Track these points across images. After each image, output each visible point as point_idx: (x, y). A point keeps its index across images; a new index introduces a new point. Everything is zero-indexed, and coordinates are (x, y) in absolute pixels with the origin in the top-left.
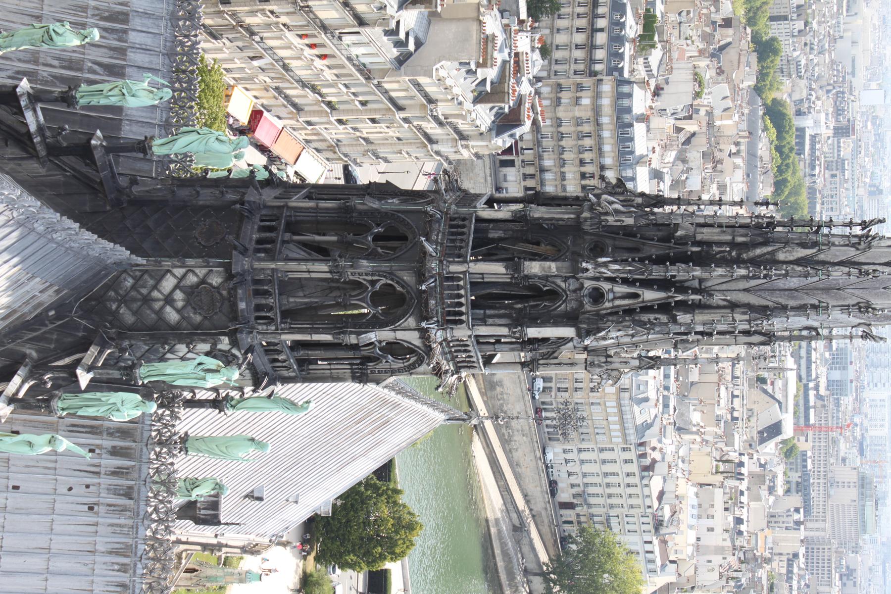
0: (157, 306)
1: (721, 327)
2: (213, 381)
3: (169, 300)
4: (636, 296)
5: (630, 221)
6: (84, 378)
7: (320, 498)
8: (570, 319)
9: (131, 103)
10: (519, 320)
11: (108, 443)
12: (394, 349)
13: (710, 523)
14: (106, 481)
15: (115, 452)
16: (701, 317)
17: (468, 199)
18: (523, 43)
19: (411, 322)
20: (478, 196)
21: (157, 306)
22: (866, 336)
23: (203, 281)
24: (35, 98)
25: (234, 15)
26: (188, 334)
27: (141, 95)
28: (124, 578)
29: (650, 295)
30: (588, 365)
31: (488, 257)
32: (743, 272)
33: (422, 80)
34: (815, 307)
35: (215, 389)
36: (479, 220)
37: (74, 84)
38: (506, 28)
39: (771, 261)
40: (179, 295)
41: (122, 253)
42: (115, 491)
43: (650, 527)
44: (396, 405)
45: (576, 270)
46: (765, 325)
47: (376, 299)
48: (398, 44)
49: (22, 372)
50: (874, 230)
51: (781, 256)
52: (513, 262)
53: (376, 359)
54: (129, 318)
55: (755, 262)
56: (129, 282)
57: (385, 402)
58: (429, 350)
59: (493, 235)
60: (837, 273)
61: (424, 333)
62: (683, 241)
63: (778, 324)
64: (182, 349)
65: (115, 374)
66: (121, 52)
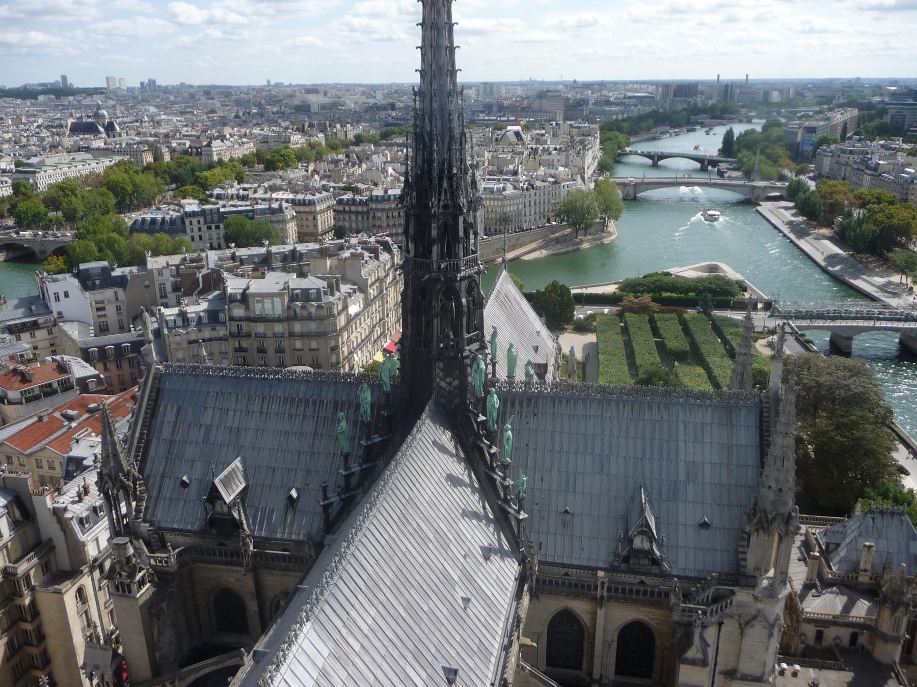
0: (452, 389)
1: (458, 154)
2: (483, 366)
3: (450, 384)
4: (446, 191)
5: (414, 194)
6: (482, 418)
7: (536, 323)
9: (369, 399)
11: (509, 408)
12: (469, 291)
13: (556, 161)
14: (524, 409)
15: (513, 406)
16: (454, 163)
18: (354, 241)
19: (457, 284)
20: (406, 257)
21: (452, 389)
23: (442, 370)
24: (368, 438)
25: (344, 360)
26: (463, 376)
27: (366, 396)
28: (564, 402)
29: (445, 185)
30: (475, 210)
31: (431, 253)
32: (435, 145)
33: (369, 282)
34: (450, 115)
35: (487, 365)
36: (415, 256)
37: (362, 422)
38: (348, 248)
39: (430, 134)
40: (448, 380)
41: (431, 403)
42: (529, 405)
43: (557, 186)
44: (499, 291)
46: (457, 136)
47: (449, 299)
48: (355, 292)
49: (479, 443)
51: (429, 129)
52: (432, 242)
53: (474, 298)
54: (458, 400)
55: (431, 140)
56: (443, 400)
57: (497, 296)
58: (470, 277)
59: (421, 250)
60: (435, 106)
61: (462, 279)
62: (423, 171)
63: (457, 131)
64: (470, 379)
65: (480, 406)
66: (350, 404)
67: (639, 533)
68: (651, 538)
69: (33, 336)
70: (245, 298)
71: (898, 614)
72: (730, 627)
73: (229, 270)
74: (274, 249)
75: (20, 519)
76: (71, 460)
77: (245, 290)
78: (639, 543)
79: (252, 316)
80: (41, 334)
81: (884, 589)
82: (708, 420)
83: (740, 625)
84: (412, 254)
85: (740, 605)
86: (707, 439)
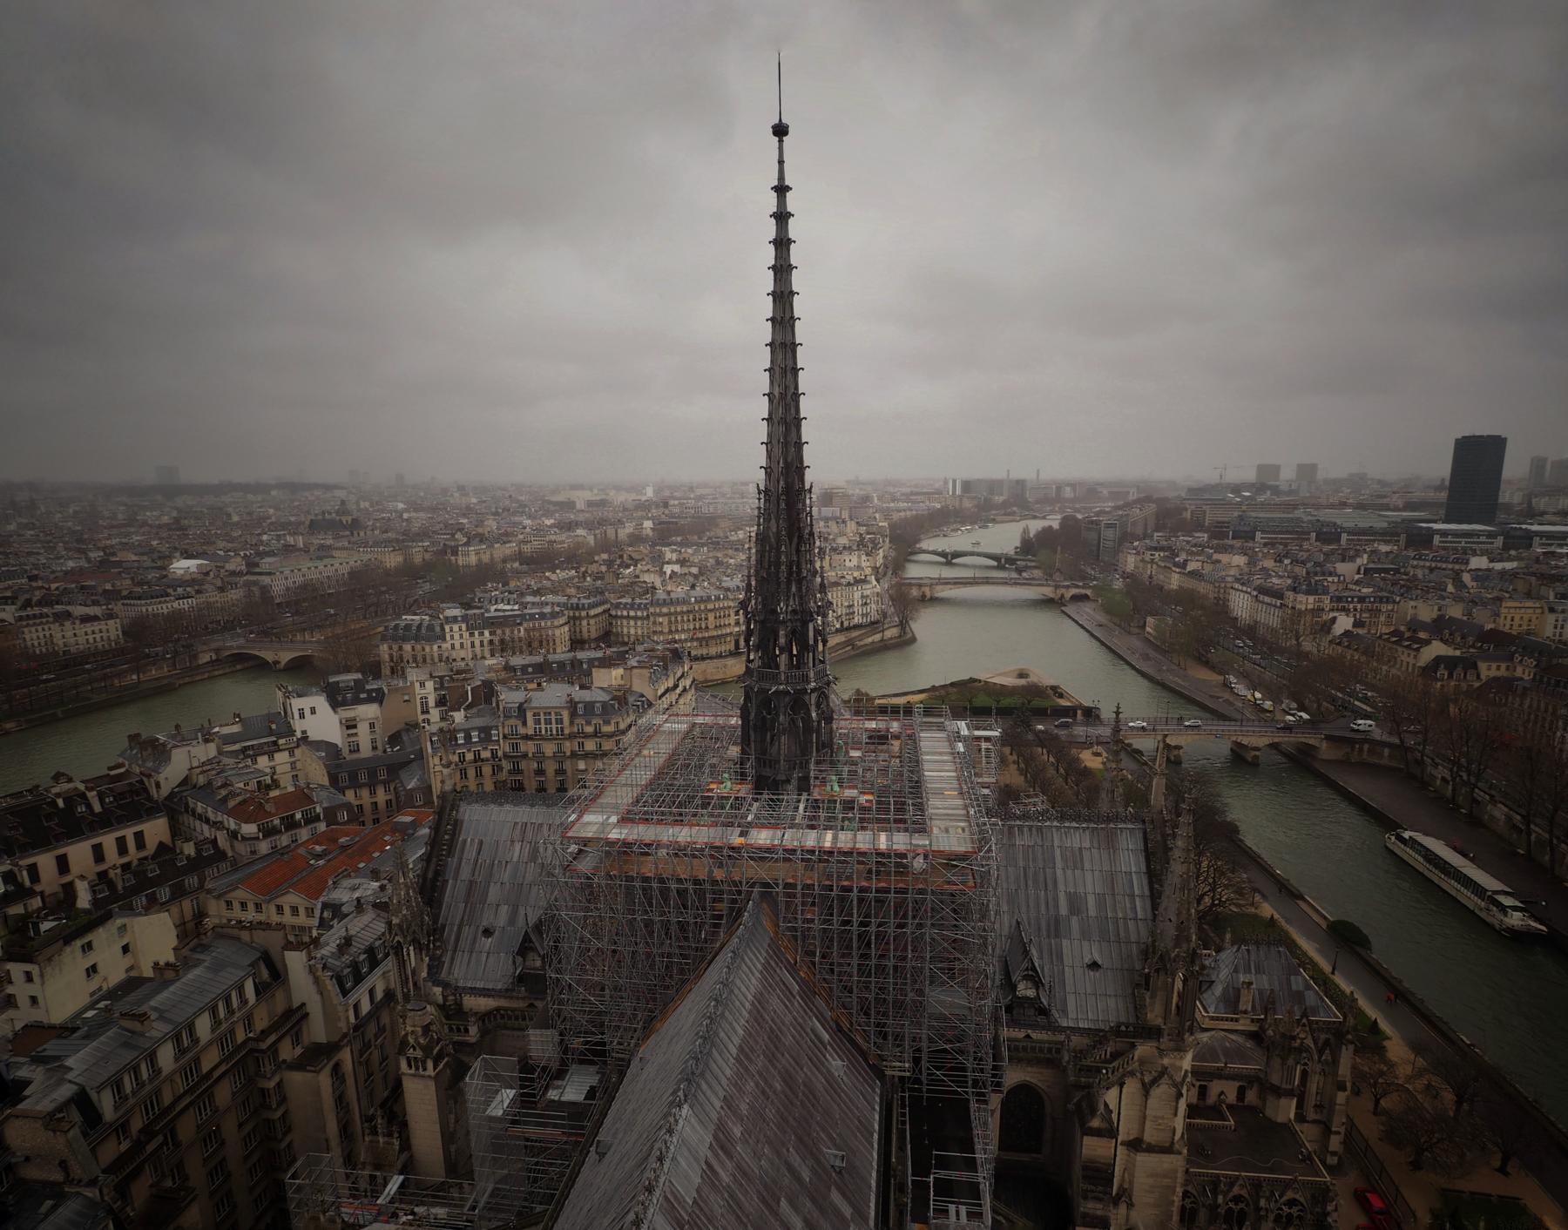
8: (805, 624)
10: (805, 647)
12: (818, 706)
17: (748, 671)
22: (810, 491)
29: (794, 589)
45: (784, 622)
50: (762, 487)
61: (813, 691)
67: (1026, 978)
68: (1037, 982)
70: (521, 710)
71: (1291, 1062)
72: (1131, 1086)
73: (503, 682)
74: (551, 657)
77: (521, 705)
78: (1025, 990)
79: (531, 732)
81: (1270, 1032)
82: (1087, 844)
83: (1143, 1084)
84: (758, 663)
85: (1142, 1062)
86: (1087, 866)
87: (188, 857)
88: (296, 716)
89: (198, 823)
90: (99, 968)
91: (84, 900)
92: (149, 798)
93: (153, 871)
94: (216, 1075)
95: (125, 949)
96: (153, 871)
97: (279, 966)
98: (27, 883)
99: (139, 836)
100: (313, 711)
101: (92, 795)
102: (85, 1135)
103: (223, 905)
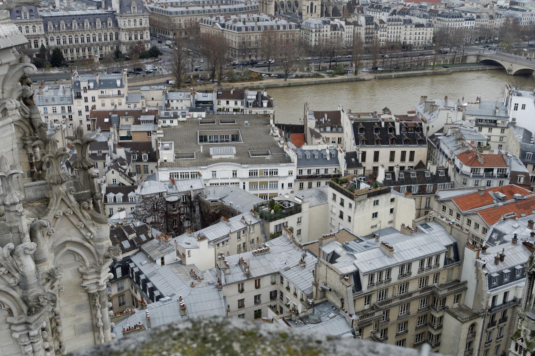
69: (490, 130)
75: (453, 259)
76: (495, 231)
80: (496, 131)
87: (431, 174)
88: (513, 108)
89: (441, 156)
90: (379, 215)
91: (381, 178)
92: (422, 135)
93: (413, 175)
94: (414, 296)
95: (392, 211)
96: (413, 175)
97: (460, 254)
98: (360, 161)
99: (412, 153)
100: (524, 107)
101: (397, 125)
102: (353, 292)
103: (442, 207)
